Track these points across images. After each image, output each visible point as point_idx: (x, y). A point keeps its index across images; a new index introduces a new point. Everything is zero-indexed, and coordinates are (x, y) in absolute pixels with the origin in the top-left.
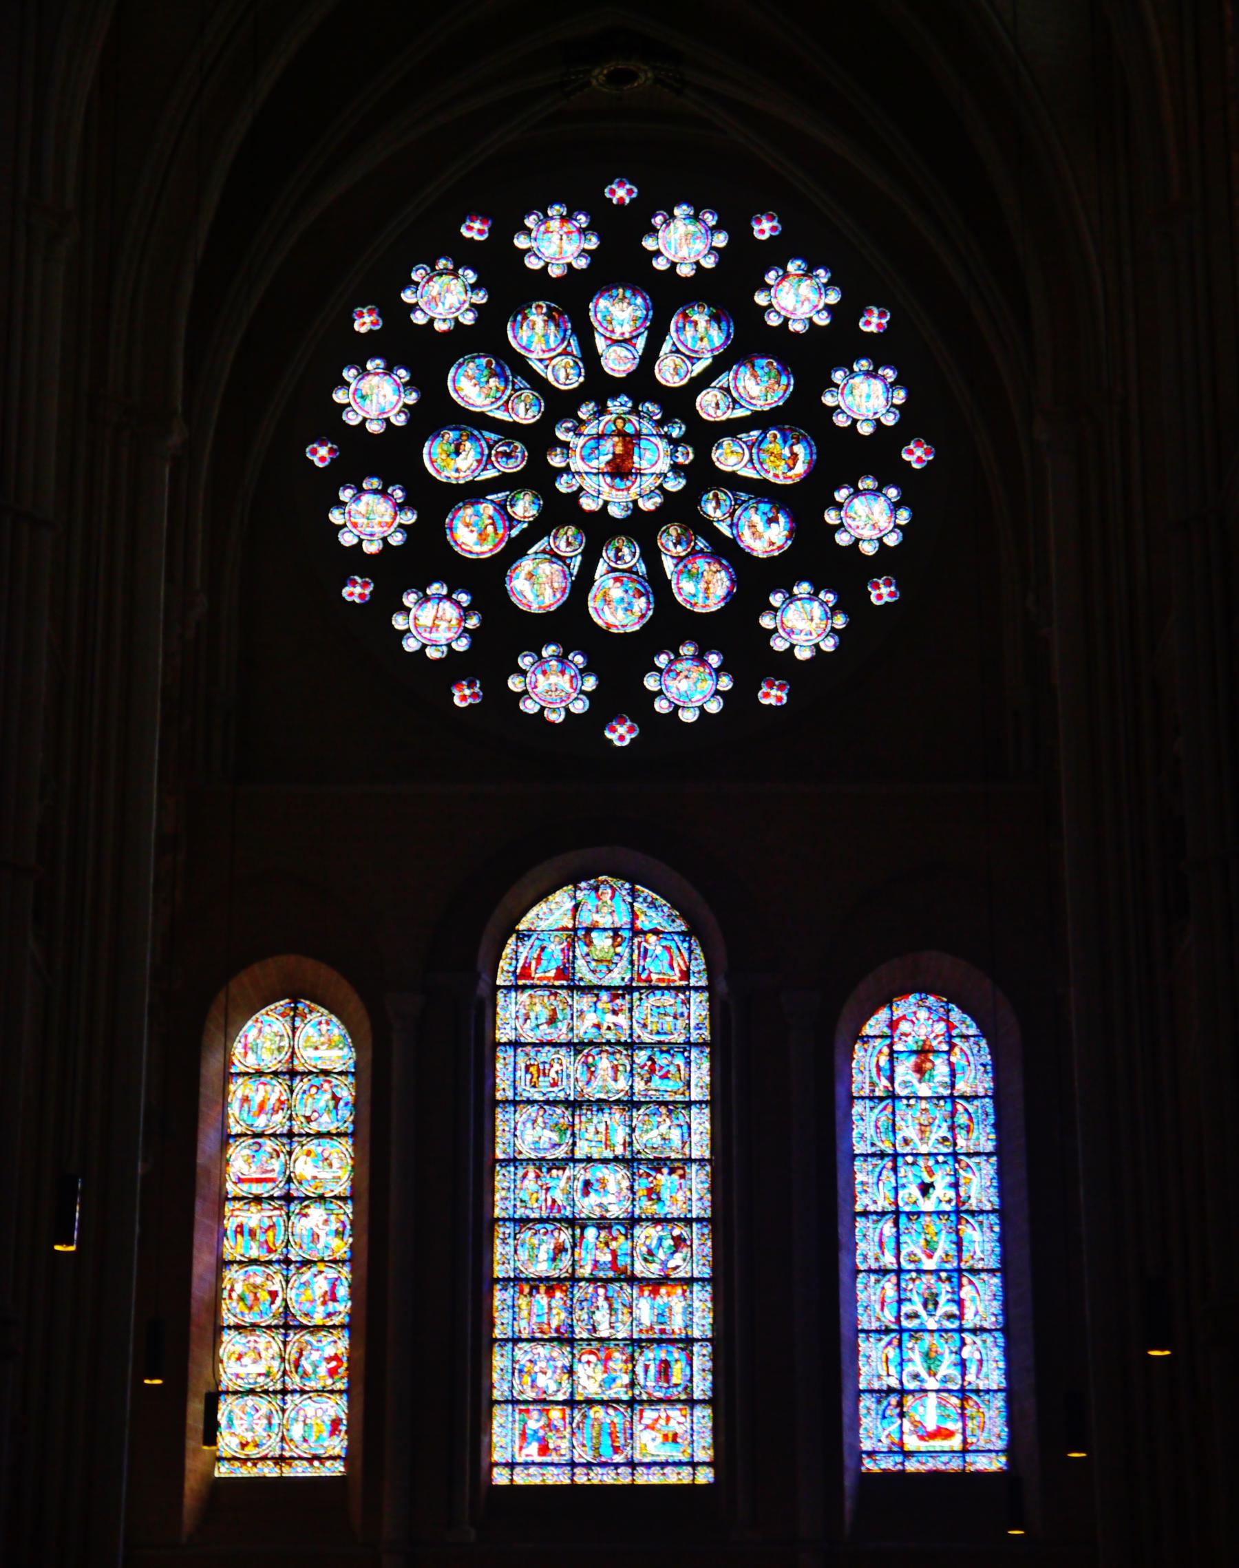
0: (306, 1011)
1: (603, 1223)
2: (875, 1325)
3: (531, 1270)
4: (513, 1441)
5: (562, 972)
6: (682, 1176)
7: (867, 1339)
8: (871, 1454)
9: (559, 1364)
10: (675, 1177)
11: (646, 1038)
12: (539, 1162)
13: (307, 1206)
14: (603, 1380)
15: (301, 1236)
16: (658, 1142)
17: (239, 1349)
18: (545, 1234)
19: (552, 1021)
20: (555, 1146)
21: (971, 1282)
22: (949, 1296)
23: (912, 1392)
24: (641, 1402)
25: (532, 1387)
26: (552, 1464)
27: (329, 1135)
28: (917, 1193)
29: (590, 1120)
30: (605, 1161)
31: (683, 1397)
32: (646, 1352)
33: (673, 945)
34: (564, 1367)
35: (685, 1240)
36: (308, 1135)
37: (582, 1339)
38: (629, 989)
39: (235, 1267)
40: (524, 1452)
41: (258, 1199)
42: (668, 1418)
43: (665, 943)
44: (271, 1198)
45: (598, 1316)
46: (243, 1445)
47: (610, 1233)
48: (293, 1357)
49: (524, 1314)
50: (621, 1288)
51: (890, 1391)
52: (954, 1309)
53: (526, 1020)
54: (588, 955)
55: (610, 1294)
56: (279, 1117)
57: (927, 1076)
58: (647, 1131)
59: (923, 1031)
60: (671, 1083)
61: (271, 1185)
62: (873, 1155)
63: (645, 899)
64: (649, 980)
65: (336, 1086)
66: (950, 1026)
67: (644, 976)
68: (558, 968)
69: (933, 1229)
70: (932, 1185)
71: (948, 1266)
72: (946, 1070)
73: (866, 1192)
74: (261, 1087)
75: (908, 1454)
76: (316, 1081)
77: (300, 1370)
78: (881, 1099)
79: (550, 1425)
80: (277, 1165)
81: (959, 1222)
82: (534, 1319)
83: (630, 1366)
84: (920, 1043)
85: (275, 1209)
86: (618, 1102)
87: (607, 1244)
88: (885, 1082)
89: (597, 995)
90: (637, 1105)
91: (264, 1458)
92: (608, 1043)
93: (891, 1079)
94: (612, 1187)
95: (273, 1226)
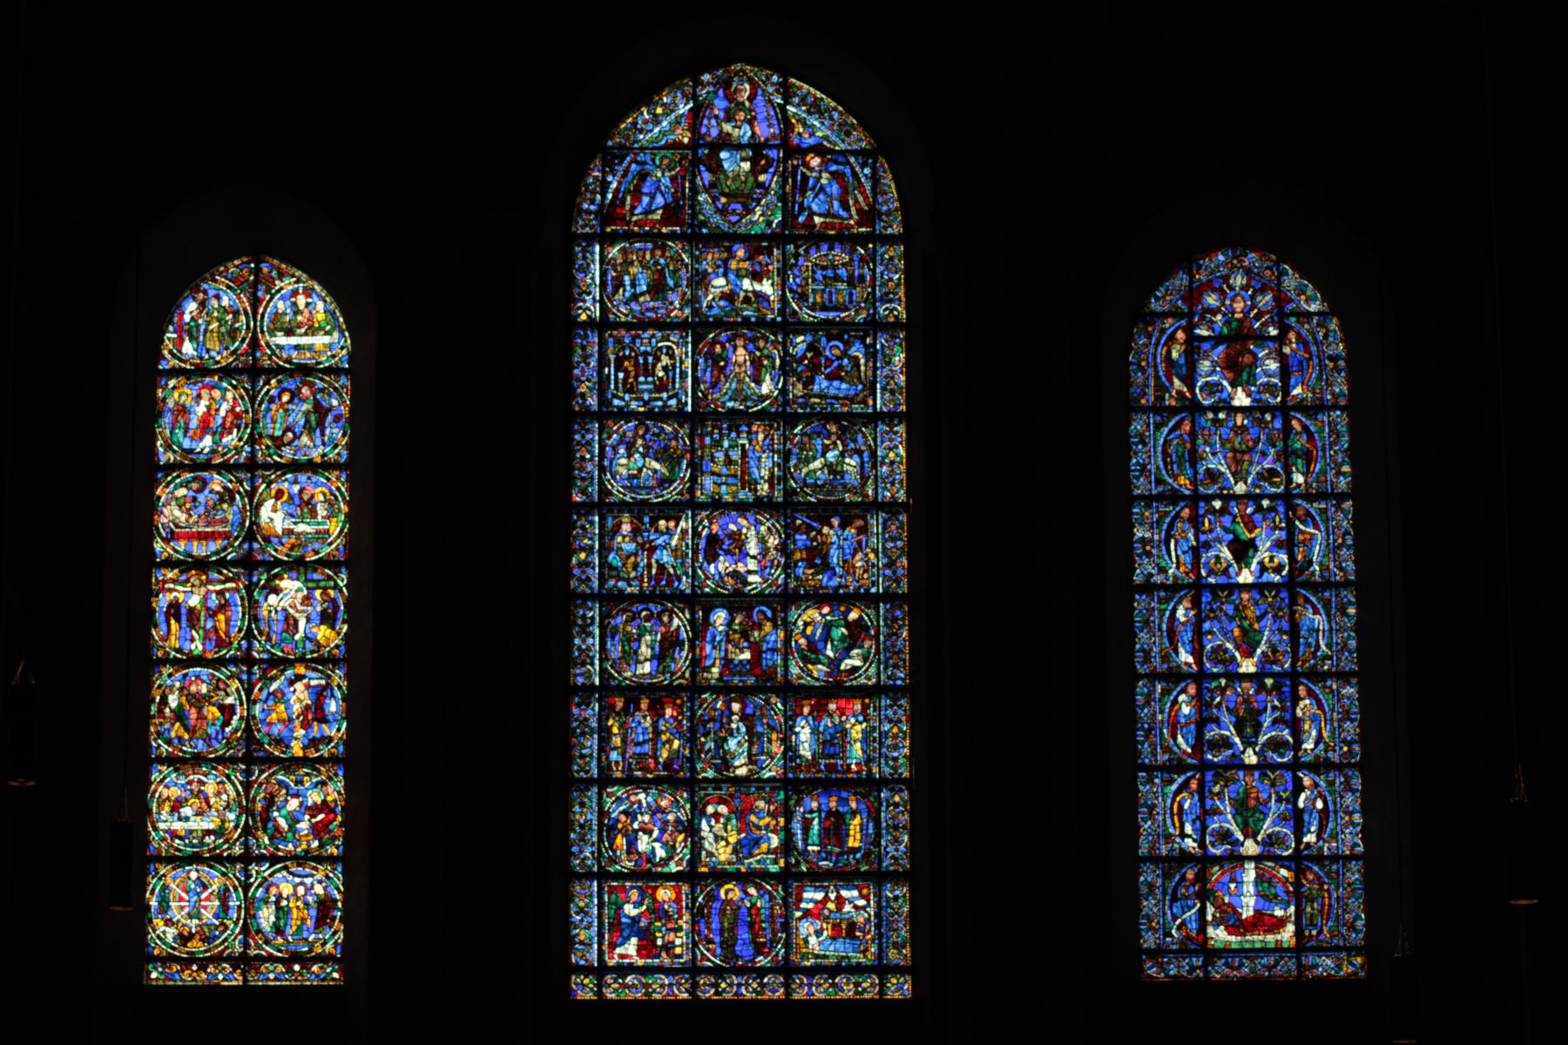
0: (274, 274)
1: (738, 600)
2: (1162, 758)
3: (628, 674)
4: (601, 936)
5: (672, 213)
6: (863, 530)
7: (1150, 781)
8: (1157, 953)
9: (671, 817)
10: (851, 531)
11: (806, 315)
12: (638, 509)
13: (277, 576)
14: (739, 842)
15: (269, 621)
16: (823, 476)
17: (175, 792)
18: (647, 619)
19: (658, 288)
20: (664, 482)
21: (1311, 694)
22: (1277, 714)
23: (1218, 860)
24: (800, 876)
25: (629, 852)
26: (661, 969)
27: (311, 467)
28: (1226, 554)
29: (717, 444)
30: (741, 507)
31: (864, 868)
32: (807, 800)
33: (848, 170)
34: (678, 821)
35: (867, 629)
36: (277, 466)
37: (706, 780)
38: (775, 239)
39: (167, 670)
40: (618, 950)
41: (202, 565)
42: (840, 901)
43: (834, 168)
44: (222, 563)
45: (732, 744)
46: (184, 939)
47: (750, 617)
48: (259, 806)
49: (617, 741)
50: (767, 701)
51: (1185, 857)
52: (1286, 734)
53: (616, 291)
54: (713, 185)
55: (749, 711)
56: (231, 439)
57: (1245, 376)
58: (807, 461)
59: (1239, 306)
60: (844, 386)
61: (220, 543)
62: (1160, 498)
63: (803, 101)
64: (809, 223)
65: (322, 390)
66: (1281, 299)
67: (801, 219)
68: (666, 207)
69: (1252, 612)
70: (1252, 545)
71: (1276, 668)
72: (1273, 366)
73: (1149, 555)
74: (204, 392)
75: (1211, 954)
76: (291, 384)
77: (270, 825)
78: (1173, 411)
79: (657, 911)
80: (230, 513)
81: (1293, 601)
82: (632, 750)
83: (782, 821)
84: (1234, 325)
85: (228, 580)
86: (762, 415)
87: (745, 635)
88: (1177, 382)
89: (729, 249)
90: (791, 420)
91: (217, 959)
92: (746, 322)
93: (1190, 381)
94: (753, 548)
95: (224, 607)
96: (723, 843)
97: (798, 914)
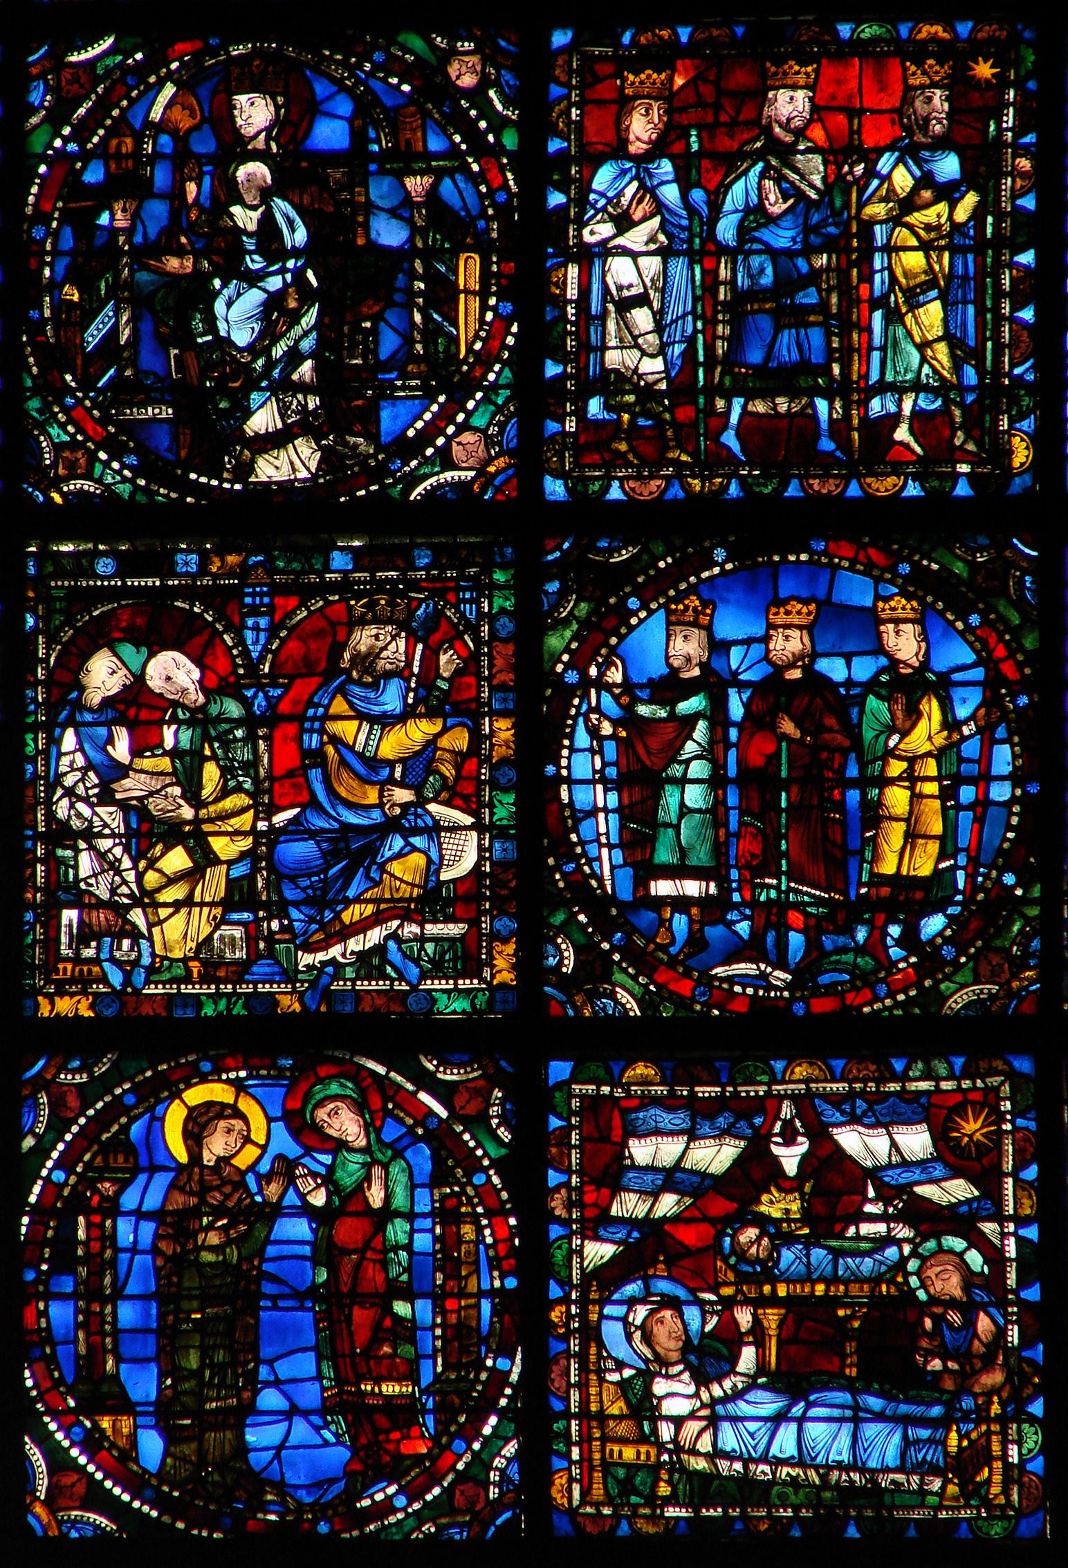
55: (330, 133)
96: (177, 860)
97: (599, 1252)
